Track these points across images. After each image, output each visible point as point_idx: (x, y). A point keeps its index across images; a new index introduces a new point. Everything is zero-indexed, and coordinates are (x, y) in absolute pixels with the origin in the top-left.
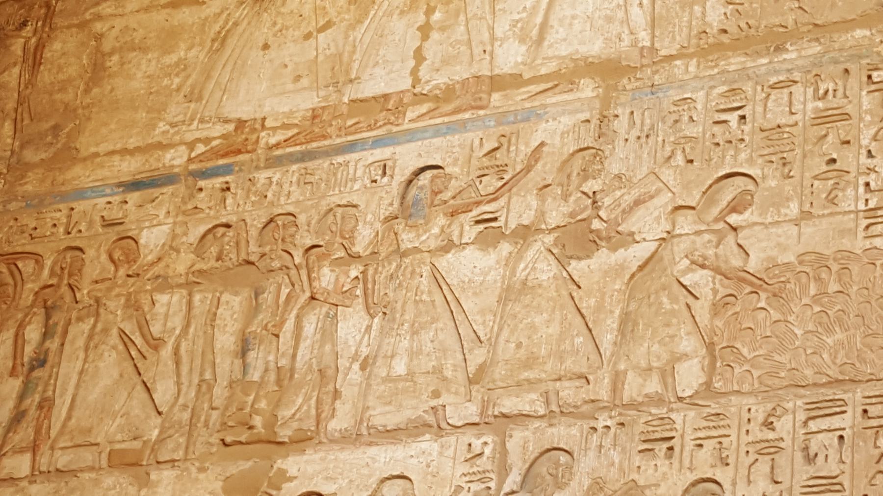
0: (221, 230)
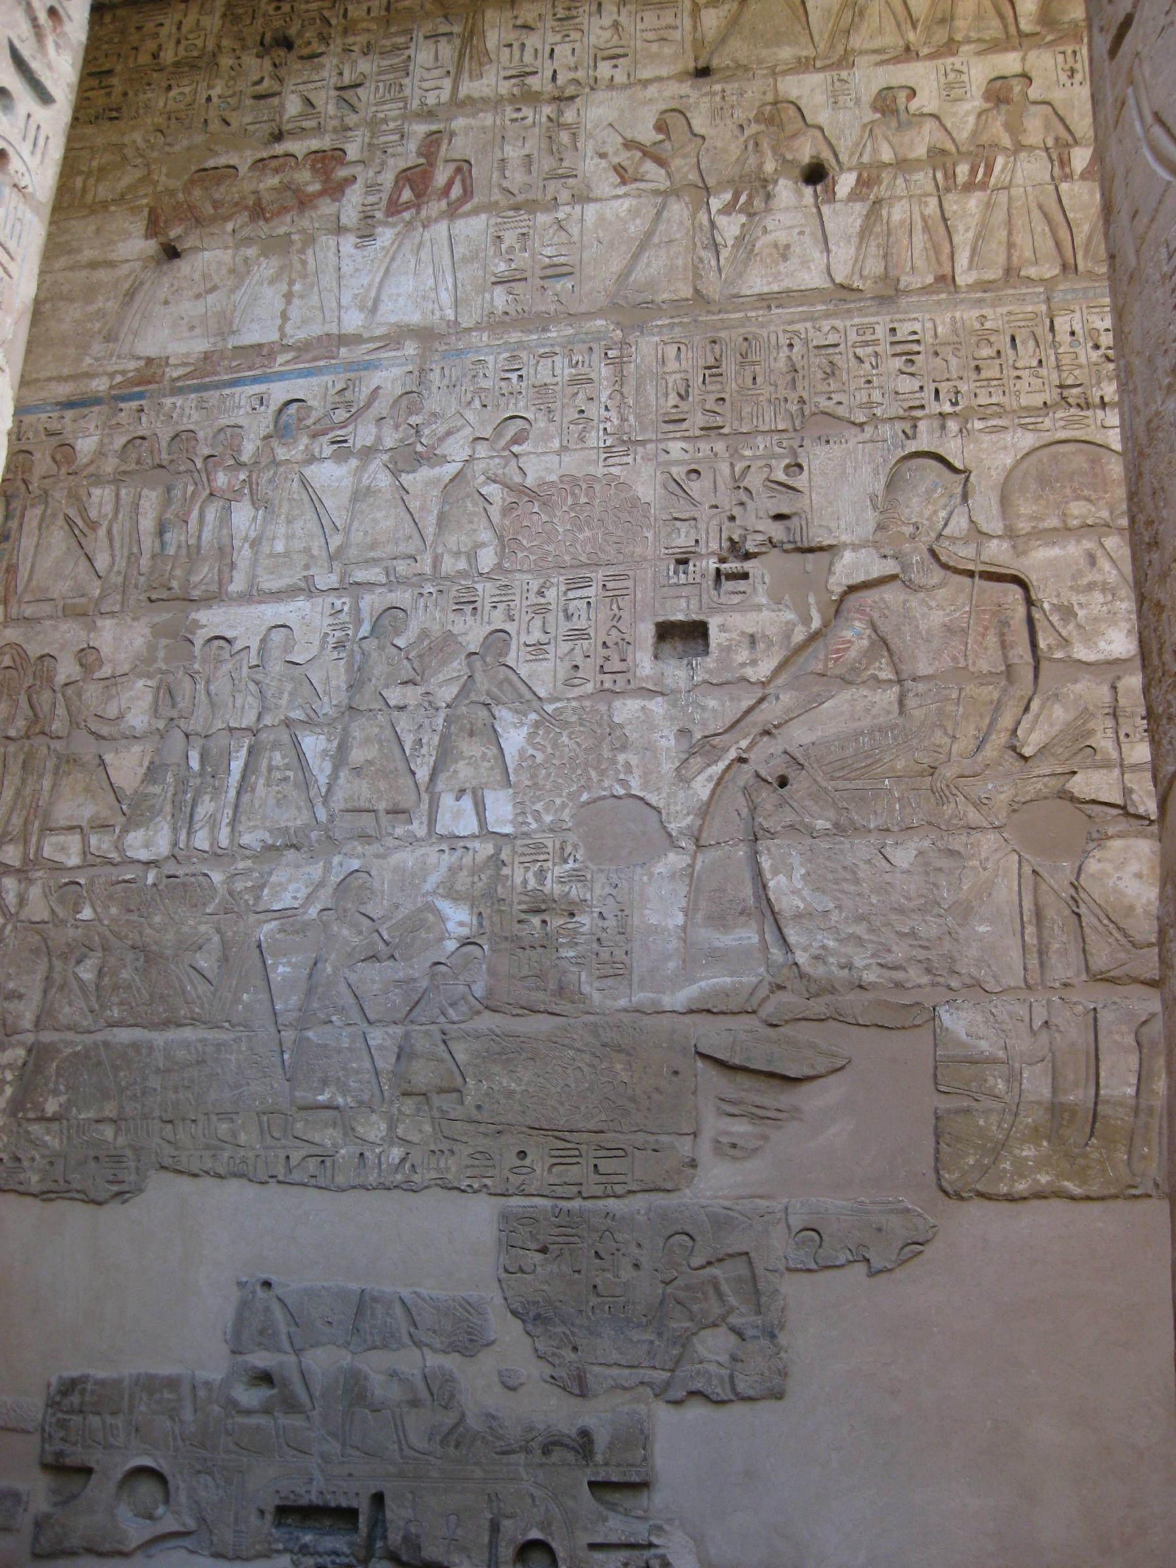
0: (139, 441)
